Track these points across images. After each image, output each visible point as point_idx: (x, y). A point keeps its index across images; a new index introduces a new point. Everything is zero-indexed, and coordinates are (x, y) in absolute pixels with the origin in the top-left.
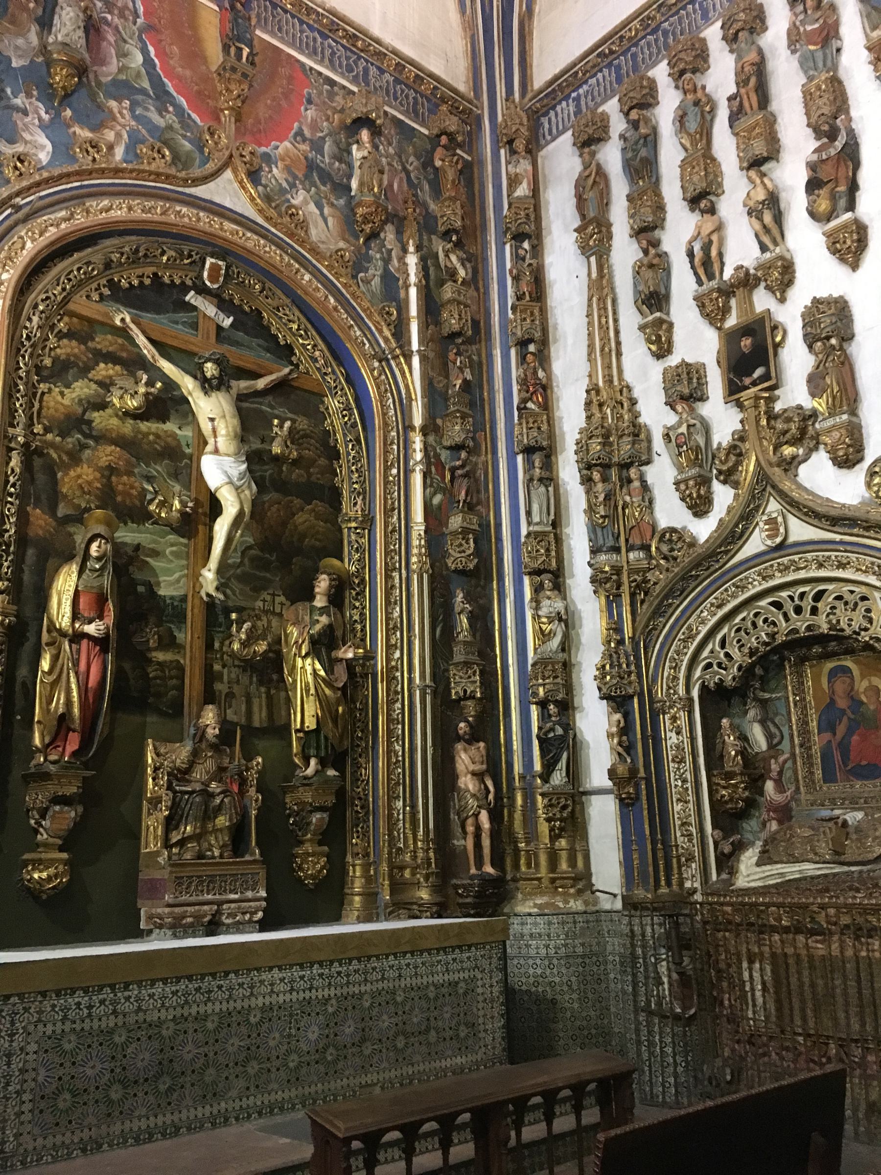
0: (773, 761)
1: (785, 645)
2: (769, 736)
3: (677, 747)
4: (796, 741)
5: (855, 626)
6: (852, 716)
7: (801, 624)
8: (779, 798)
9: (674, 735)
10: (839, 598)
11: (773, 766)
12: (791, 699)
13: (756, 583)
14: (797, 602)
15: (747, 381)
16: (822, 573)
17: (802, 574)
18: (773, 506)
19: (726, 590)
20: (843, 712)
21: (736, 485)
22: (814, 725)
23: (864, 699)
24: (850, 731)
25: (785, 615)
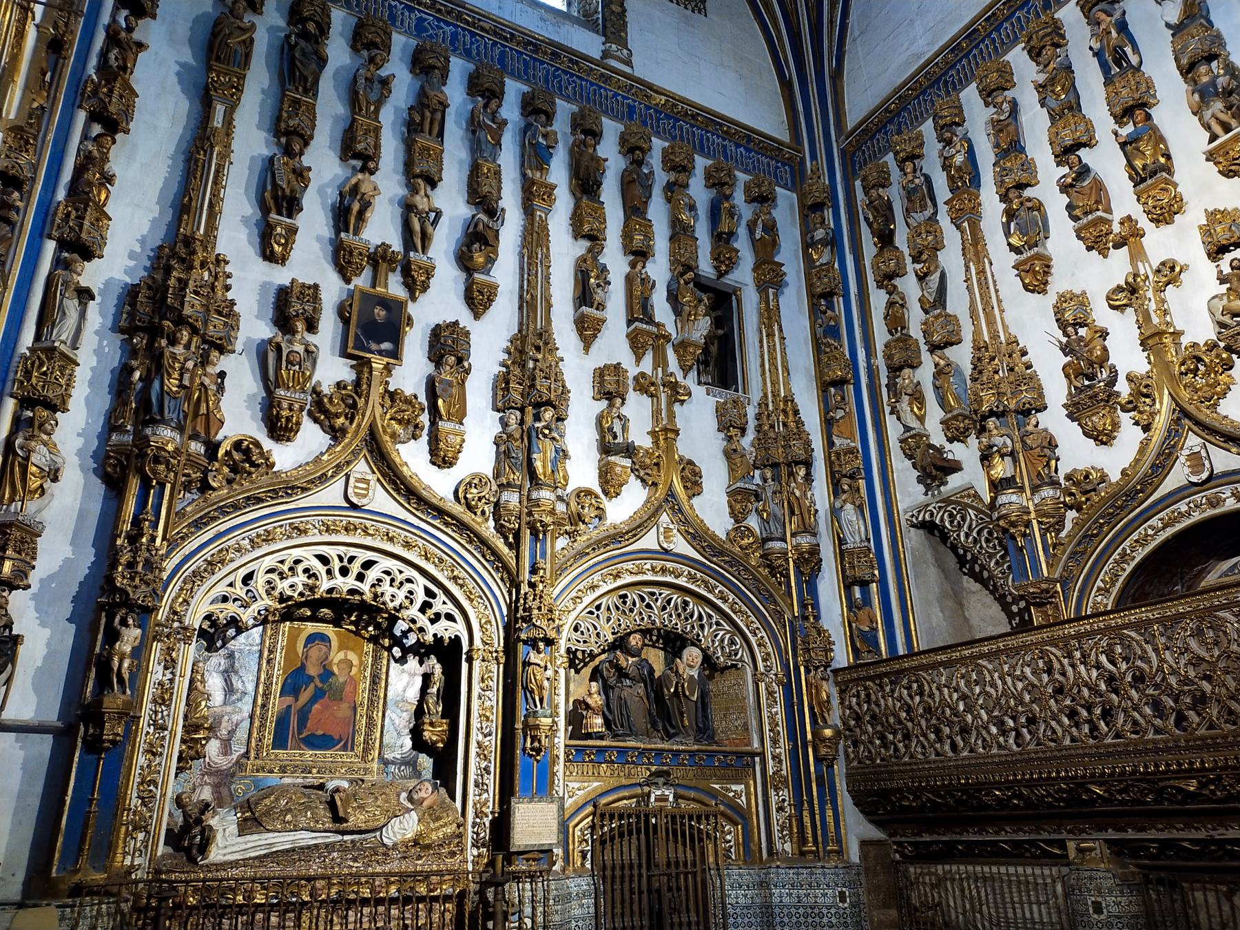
0: (226, 718)
1: (322, 602)
2: (229, 689)
3: (161, 684)
4: (260, 701)
5: (397, 603)
6: (320, 685)
7: (345, 584)
8: (223, 762)
9: (160, 669)
10: (387, 573)
11: (224, 724)
12: (266, 654)
13: (316, 531)
14: (345, 563)
15: (374, 346)
16: (388, 547)
17: (368, 541)
18: (361, 468)
19: (281, 526)
20: (311, 679)
21: (336, 434)
22: (277, 688)
23: (335, 669)
24: (314, 699)
25: (329, 572)
